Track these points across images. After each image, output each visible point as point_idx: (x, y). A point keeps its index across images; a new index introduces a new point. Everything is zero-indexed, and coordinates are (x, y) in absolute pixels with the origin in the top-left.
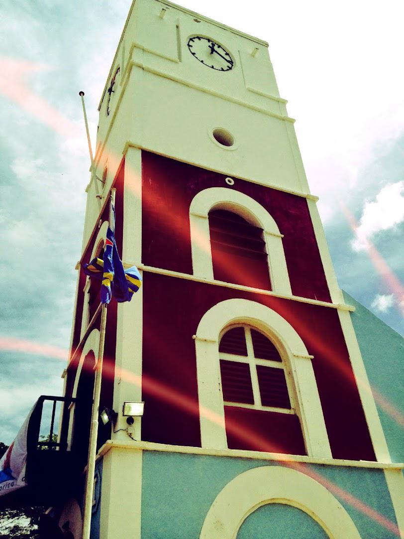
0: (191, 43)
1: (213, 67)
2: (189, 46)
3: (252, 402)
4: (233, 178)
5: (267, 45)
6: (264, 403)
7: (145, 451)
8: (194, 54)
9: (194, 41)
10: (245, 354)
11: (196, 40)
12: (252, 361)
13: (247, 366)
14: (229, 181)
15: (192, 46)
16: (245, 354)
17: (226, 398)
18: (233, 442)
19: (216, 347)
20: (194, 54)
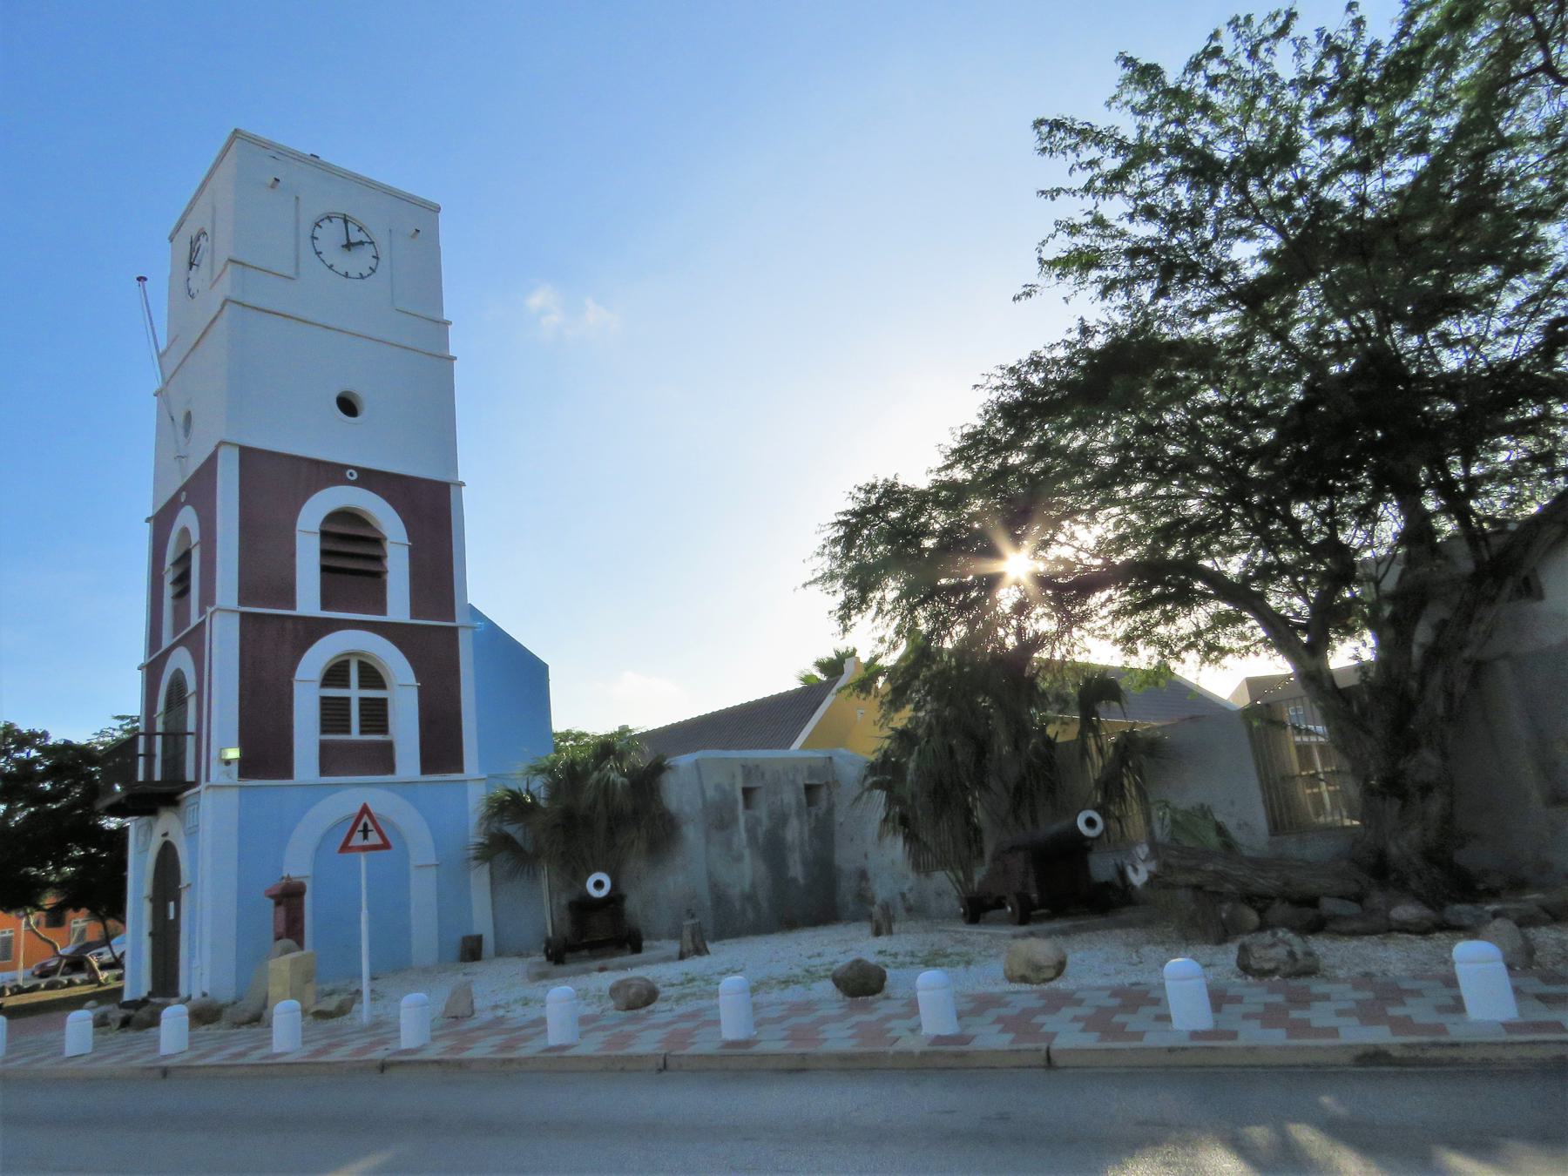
0: (318, 232)
1: (346, 275)
2: (313, 238)
3: (347, 730)
4: (356, 468)
5: (438, 209)
6: (362, 732)
7: (241, 787)
8: (318, 253)
9: (320, 227)
10: (346, 685)
11: (326, 224)
12: (354, 693)
13: (347, 700)
14: (351, 475)
15: (317, 238)
16: (346, 685)
17: (324, 731)
18: (324, 770)
19: (318, 684)
20: (318, 253)
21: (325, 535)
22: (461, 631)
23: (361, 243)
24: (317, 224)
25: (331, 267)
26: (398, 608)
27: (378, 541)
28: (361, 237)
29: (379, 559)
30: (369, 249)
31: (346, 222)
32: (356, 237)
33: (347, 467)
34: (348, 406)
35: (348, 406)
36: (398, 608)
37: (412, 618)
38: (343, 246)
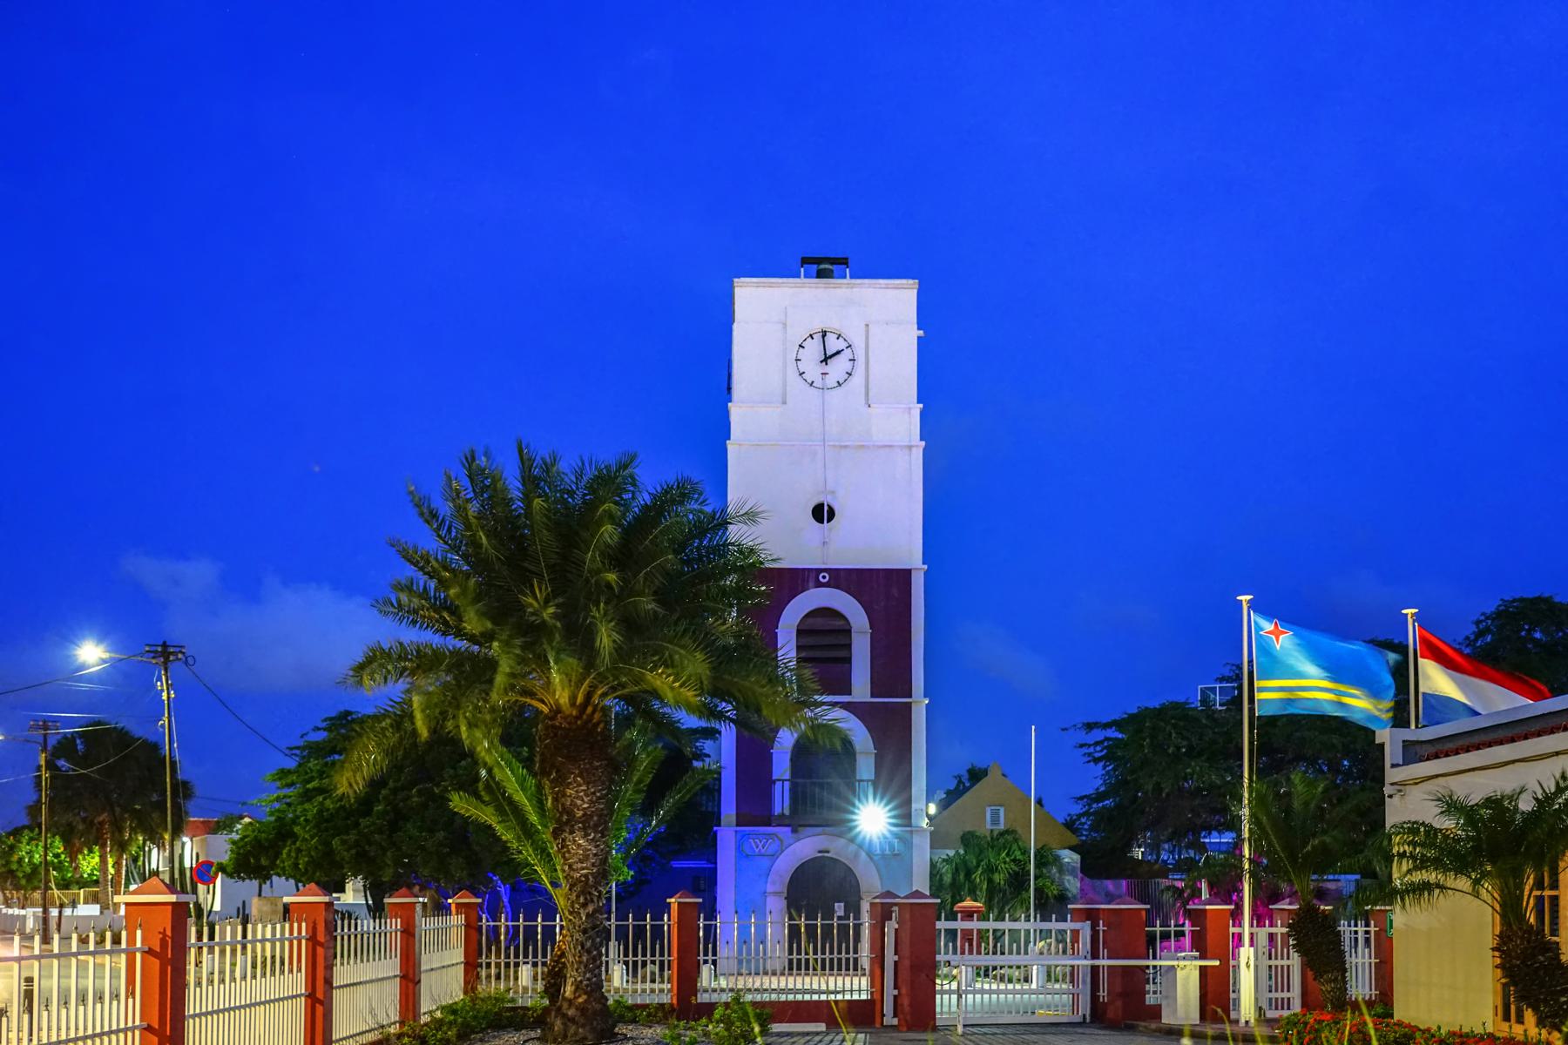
14: (824, 577)
21: (800, 632)
22: (913, 705)
23: (838, 353)
24: (800, 346)
25: (811, 384)
26: (861, 689)
27: (847, 631)
28: (841, 345)
29: (849, 646)
30: (847, 354)
31: (824, 336)
32: (833, 344)
33: (820, 571)
34: (822, 513)
35: (822, 513)
36: (861, 689)
37: (872, 696)
38: (821, 362)
